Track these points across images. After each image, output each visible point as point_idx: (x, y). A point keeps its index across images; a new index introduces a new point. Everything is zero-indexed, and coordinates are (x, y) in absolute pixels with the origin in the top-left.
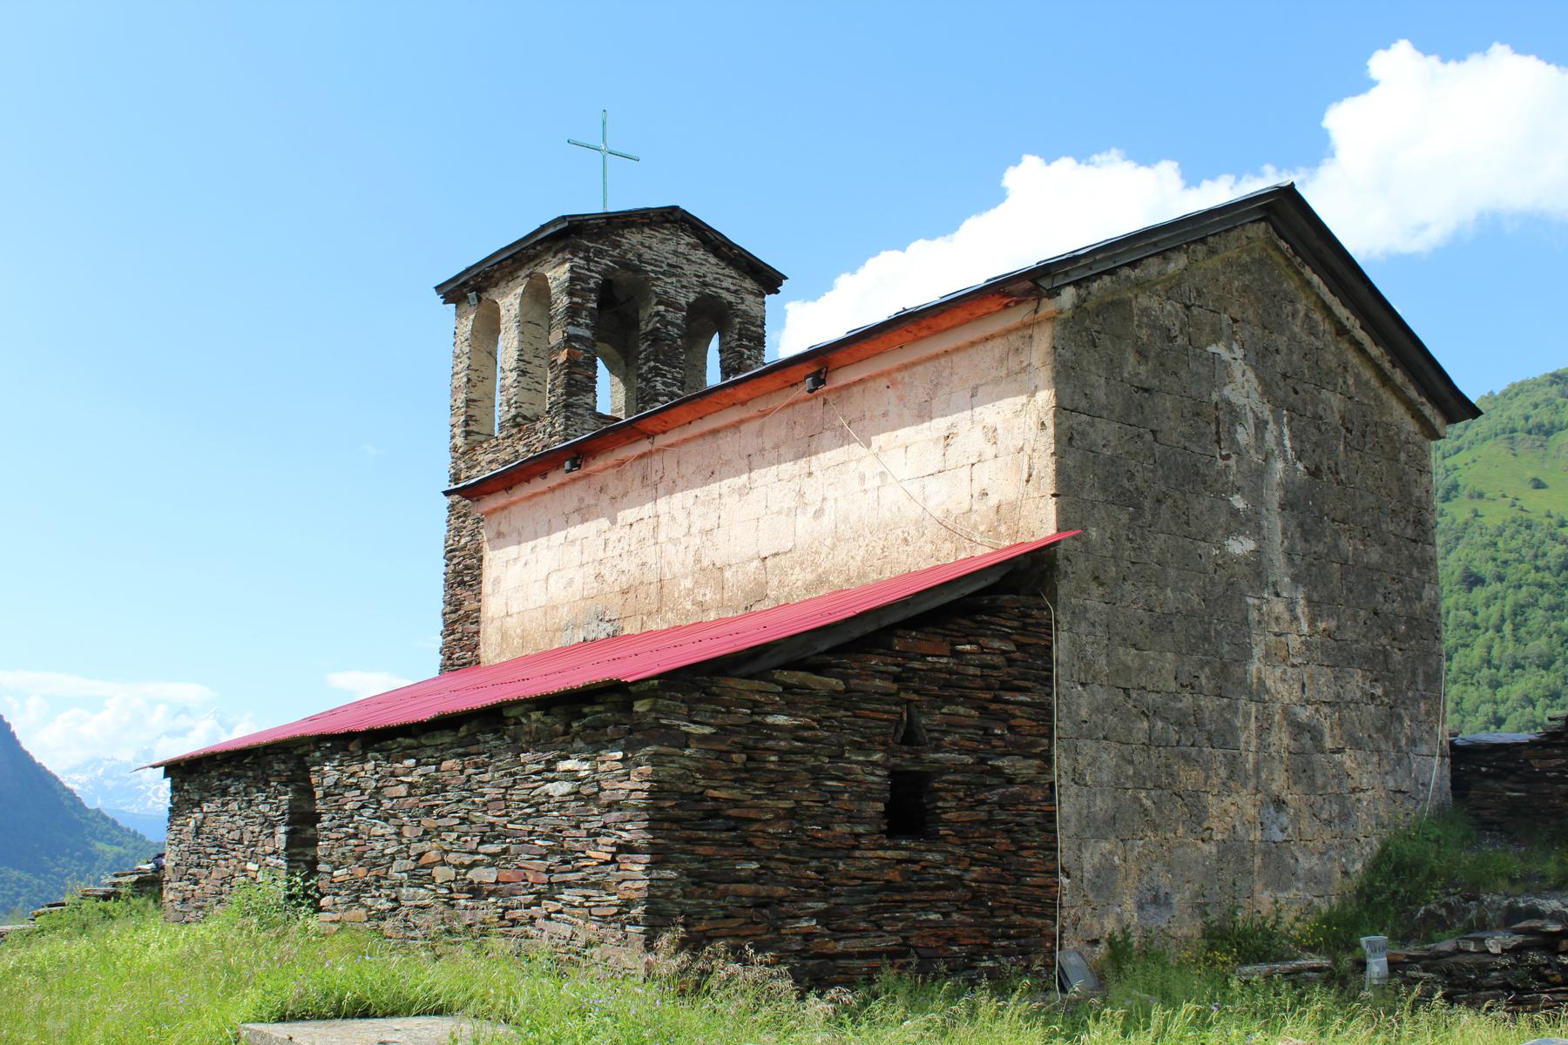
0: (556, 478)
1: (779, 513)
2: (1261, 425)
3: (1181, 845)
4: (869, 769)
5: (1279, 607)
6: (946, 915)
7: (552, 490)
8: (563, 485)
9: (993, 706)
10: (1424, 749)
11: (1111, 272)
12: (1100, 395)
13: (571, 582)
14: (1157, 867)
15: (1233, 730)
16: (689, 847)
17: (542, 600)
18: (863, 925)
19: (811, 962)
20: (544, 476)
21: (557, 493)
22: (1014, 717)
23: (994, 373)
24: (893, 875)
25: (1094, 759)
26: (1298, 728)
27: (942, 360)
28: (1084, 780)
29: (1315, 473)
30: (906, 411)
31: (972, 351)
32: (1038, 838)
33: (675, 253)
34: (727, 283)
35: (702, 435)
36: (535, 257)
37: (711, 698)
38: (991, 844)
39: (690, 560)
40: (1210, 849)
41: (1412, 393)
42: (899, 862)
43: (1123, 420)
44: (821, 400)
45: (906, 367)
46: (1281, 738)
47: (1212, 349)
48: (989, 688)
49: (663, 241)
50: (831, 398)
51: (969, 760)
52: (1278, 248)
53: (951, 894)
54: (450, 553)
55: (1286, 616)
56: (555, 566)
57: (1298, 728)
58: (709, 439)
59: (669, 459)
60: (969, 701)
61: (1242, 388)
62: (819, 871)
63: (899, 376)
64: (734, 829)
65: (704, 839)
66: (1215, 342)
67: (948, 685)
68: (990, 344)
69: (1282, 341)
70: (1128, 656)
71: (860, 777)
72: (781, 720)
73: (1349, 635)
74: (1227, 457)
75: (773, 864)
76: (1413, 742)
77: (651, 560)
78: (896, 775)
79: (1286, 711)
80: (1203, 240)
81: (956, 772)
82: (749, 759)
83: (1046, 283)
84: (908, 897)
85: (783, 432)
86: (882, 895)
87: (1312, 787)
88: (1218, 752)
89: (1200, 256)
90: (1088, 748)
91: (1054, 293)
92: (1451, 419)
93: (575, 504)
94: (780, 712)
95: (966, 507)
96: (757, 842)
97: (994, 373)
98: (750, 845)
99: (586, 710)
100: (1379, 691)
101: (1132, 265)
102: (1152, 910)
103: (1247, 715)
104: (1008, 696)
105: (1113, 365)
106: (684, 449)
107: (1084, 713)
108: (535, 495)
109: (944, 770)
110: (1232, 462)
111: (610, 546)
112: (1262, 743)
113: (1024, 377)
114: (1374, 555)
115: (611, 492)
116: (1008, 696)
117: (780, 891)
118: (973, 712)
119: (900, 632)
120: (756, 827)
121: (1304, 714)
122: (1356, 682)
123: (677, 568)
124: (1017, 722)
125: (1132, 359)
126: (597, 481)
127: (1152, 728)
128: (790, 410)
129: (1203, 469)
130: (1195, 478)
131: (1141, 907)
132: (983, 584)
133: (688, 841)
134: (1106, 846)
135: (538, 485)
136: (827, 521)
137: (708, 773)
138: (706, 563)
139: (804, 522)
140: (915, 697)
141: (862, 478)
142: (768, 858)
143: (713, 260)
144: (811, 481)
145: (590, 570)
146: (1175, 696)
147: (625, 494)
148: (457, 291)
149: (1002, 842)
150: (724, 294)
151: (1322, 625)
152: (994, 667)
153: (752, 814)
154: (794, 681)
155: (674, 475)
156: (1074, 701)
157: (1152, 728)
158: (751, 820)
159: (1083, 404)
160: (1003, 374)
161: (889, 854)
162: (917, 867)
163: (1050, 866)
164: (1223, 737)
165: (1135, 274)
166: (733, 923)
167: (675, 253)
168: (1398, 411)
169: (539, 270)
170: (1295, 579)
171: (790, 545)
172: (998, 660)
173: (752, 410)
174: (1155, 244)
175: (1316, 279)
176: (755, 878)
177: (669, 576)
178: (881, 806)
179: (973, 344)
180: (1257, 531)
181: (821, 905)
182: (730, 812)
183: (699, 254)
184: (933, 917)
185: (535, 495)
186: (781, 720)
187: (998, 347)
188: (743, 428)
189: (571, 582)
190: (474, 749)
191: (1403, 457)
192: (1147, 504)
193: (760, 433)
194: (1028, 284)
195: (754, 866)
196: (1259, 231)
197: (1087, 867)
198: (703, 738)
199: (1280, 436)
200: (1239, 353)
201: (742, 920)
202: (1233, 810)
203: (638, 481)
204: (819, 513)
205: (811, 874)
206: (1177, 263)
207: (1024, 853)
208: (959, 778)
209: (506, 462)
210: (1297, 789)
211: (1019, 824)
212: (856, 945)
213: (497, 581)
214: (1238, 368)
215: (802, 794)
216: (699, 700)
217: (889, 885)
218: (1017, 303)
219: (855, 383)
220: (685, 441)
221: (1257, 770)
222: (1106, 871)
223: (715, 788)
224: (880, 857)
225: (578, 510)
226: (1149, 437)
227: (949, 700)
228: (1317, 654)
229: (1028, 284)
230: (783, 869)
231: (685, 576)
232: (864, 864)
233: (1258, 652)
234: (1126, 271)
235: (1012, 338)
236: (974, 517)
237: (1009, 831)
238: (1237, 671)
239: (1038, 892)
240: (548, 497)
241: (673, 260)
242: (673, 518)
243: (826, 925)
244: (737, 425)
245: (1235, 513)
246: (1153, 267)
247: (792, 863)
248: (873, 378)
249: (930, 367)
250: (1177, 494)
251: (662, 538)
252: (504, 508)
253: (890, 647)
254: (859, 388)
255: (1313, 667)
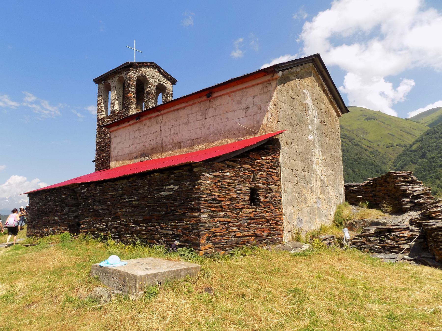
0: (131, 122)
1: (197, 128)
2: (313, 110)
3: (304, 208)
4: (246, 187)
5: (317, 153)
6: (262, 225)
7: (130, 125)
8: (133, 124)
9: (269, 173)
10: (340, 186)
11: (288, 69)
12: (286, 98)
13: (136, 147)
14: (300, 213)
15: (311, 181)
16: (209, 208)
17: (128, 152)
18: (246, 229)
19: (236, 239)
20: (129, 122)
21: (132, 126)
22: (273, 175)
23: (260, 92)
24: (251, 215)
25: (288, 186)
26: (322, 181)
27: (244, 90)
28: (287, 191)
29: (321, 122)
30: (234, 103)
31: (253, 87)
32: (279, 206)
33: (153, 73)
34: (165, 81)
35: (174, 110)
36: (120, 72)
37: (212, 168)
38: (269, 207)
39: (171, 140)
40: (308, 208)
41: (336, 106)
42: (253, 212)
43: (290, 105)
44: (209, 101)
45: (233, 92)
46: (319, 183)
47: (304, 91)
48: (268, 168)
49: (150, 70)
50: (212, 100)
51: (265, 186)
52: (314, 69)
53: (262, 220)
54: (97, 144)
55: (318, 155)
56: (131, 143)
57: (322, 181)
58: (176, 112)
59: (164, 117)
60: (264, 171)
61: (309, 101)
62: (237, 214)
63: (231, 94)
64: (218, 203)
65: (213, 206)
66: (304, 89)
67: (260, 167)
68: (258, 85)
69: (315, 91)
70: (292, 161)
71: (244, 190)
72: (228, 174)
73: (328, 160)
74: (307, 116)
75: (227, 213)
76: (339, 185)
77: (160, 142)
78: (251, 189)
79: (320, 177)
80: (302, 65)
81: (263, 189)
82: (222, 184)
83: (276, 69)
84: (255, 221)
85: (197, 109)
86: (249, 221)
87: (324, 195)
88: (309, 186)
89: (302, 69)
90: (287, 183)
91: (278, 72)
92: (342, 113)
93: (137, 128)
94: (228, 172)
95: (252, 125)
96: (224, 207)
97: (260, 92)
98: (222, 207)
99: (175, 172)
100: (333, 173)
101: (291, 68)
102: (299, 223)
103: (313, 177)
104: (271, 170)
105: (288, 93)
106: (169, 113)
107: (286, 175)
108: (125, 127)
109: (261, 189)
110: (308, 117)
111: (147, 138)
112: (316, 184)
113: (268, 93)
114: (331, 142)
115: (147, 125)
116: (271, 170)
117: (229, 220)
118: (265, 174)
119: (251, 153)
120: (223, 202)
121: (322, 177)
122: (329, 171)
123: (167, 143)
124: (273, 177)
125: (291, 91)
126: (144, 123)
127: (298, 179)
128: (199, 104)
129: (304, 119)
130: (303, 122)
131: (297, 223)
132: (263, 143)
133: (209, 206)
134: (291, 208)
135: (127, 124)
136: (211, 130)
137: (213, 188)
138: (176, 141)
139: (204, 130)
140: (254, 169)
141: (221, 119)
142: (226, 211)
143: (161, 76)
144: (207, 120)
145: (142, 145)
146: (301, 172)
147: (152, 125)
148: (98, 81)
149: (272, 207)
150: (164, 84)
151: (324, 157)
152: (269, 163)
153: (223, 199)
154: (230, 164)
155: (166, 120)
156: (284, 172)
157: (298, 179)
158: (222, 201)
159: (283, 100)
160: (262, 92)
161: (251, 210)
162: (256, 213)
163: (281, 213)
164: (309, 183)
165: (292, 70)
166: (219, 229)
167: (153, 73)
168: (333, 111)
169: (121, 75)
170: (319, 146)
171: (200, 136)
172: (269, 161)
173: (190, 103)
174: (294, 64)
175: (321, 77)
176: (224, 217)
177: (165, 145)
178: (249, 197)
179: (253, 86)
180: (313, 135)
181: (238, 223)
182: (218, 199)
183: (158, 74)
184: (260, 226)
185: (125, 127)
186: (228, 174)
187: (260, 87)
188: (186, 108)
189: (136, 147)
190: (135, 184)
191: (335, 120)
192: (295, 126)
193: (191, 109)
194: (273, 69)
195: (223, 213)
196: (311, 64)
197: (288, 213)
198: (211, 179)
199: (316, 113)
200: (308, 93)
201: (221, 228)
202: (312, 199)
203: (155, 123)
204: (209, 128)
205: (235, 215)
206: (299, 69)
207: (276, 209)
208: (263, 190)
209: (112, 121)
210: (322, 195)
211: (275, 202)
212: (245, 234)
213: (115, 148)
214: (308, 95)
215: (232, 194)
216: (210, 168)
217: (251, 218)
218: (268, 74)
219: (218, 96)
220: (169, 112)
221: (315, 190)
222: (291, 214)
223: (214, 192)
224: (248, 211)
225: (138, 130)
226: (294, 110)
227: (260, 171)
228: (323, 164)
229: (273, 69)
230: (230, 214)
231: (170, 145)
232: (245, 212)
233: (314, 162)
234: (290, 69)
235: (265, 84)
236: (255, 128)
237: (273, 204)
238: (311, 166)
239: (279, 219)
240: (129, 127)
241: (153, 75)
242: (166, 131)
243: (238, 229)
244: (184, 108)
245: (309, 130)
246: (294, 69)
247: (231, 212)
248: (224, 95)
249: (241, 92)
250: (300, 124)
251: (163, 135)
252: (116, 130)
253: (249, 157)
254: (220, 97)
255: (322, 167)
